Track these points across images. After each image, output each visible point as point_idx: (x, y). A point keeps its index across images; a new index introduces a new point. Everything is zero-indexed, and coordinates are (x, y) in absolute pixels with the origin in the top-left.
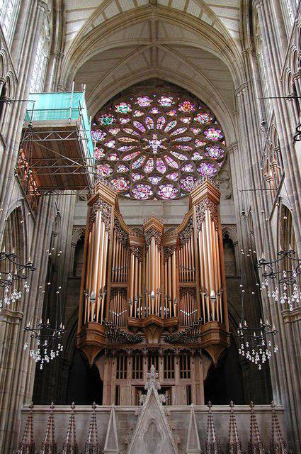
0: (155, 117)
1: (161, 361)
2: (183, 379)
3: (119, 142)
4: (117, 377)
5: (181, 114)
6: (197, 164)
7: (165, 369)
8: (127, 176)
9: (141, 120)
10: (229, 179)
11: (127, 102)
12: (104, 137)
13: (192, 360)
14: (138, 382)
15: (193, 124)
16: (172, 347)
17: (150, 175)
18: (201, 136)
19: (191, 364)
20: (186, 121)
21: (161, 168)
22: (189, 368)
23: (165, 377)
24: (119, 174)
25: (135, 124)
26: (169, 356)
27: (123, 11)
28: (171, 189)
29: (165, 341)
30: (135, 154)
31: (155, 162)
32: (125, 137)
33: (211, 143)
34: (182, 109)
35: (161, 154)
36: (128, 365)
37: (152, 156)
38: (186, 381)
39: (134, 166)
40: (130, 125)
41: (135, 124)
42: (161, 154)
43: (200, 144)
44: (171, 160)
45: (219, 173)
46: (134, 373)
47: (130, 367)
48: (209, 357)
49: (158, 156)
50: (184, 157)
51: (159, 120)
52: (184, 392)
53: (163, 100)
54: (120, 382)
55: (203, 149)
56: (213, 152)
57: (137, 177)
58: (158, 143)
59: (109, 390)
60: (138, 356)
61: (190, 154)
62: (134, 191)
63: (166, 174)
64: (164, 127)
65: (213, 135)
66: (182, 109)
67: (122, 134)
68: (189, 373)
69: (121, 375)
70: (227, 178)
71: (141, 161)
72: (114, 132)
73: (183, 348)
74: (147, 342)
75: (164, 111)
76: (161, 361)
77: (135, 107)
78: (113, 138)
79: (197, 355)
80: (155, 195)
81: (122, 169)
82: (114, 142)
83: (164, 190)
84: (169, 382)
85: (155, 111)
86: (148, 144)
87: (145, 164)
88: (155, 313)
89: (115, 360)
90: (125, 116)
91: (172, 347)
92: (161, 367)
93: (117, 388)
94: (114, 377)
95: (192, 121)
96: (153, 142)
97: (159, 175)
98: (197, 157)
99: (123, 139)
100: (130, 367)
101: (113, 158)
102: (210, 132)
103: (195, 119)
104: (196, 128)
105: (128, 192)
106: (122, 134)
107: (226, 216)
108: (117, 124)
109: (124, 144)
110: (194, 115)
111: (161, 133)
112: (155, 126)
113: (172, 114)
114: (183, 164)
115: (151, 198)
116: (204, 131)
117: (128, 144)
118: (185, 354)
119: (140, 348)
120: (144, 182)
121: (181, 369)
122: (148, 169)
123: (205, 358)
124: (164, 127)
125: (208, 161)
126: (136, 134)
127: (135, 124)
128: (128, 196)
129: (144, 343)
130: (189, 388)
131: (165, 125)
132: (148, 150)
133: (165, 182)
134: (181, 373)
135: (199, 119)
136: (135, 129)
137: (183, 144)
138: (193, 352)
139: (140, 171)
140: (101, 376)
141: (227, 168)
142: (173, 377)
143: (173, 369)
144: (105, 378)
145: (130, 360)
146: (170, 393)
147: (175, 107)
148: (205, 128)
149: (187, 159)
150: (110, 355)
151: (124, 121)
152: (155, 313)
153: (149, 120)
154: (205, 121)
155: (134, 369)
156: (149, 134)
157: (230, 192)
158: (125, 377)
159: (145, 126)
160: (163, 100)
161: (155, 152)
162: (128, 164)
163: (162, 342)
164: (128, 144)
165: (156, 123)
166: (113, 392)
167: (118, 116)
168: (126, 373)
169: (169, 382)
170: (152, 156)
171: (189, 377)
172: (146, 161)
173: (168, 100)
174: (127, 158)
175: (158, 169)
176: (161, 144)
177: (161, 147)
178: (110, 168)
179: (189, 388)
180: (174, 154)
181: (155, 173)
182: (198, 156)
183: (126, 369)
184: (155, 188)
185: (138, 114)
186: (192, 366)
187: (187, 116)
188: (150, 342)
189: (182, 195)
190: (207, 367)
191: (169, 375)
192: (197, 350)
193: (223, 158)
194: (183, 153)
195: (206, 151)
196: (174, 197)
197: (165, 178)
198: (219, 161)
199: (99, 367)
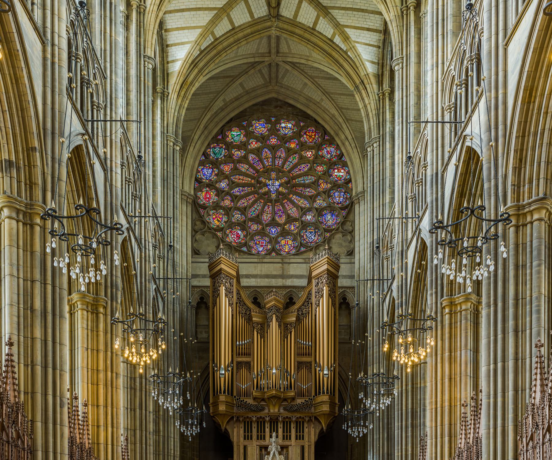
0: (273, 149)
1: (280, 425)
2: (298, 441)
3: (233, 183)
4: (245, 439)
5: (303, 146)
6: (320, 212)
7: (284, 432)
8: (243, 226)
9: (258, 152)
10: (352, 232)
11: (241, 127)
12: (216, 175)
13: (306, 425)
14: (262, 443)
15: (317, 159)
16: (289, 415)
17: (267, 225)
18: (327, 174)
19: (305, 428)
20: (309, 154)
22: (303, 432)
23: (284, 439)
24: (235, 223)
25: (251, 157)
26: (287, 423)
27: (236, 25)
28: (290, 242)
29: (285, 409)
30: (252, 198)
33: (336, 186)
34: (305, 138)
35: (281, 197)
36: (253, 429)
37: (271, 201)
38: (301, 442)
39: (252, 213)
40: (244, 159)
41: (250, 159)
42: (281, 197)
43: (323, 186)
44: (291, 206)
45: (343, 223)
46: (258, 436)
47: (254, 430)
48: (320, 422)
49: (277, 201)
50: (306, 202)
51: (279, 154)
52: (299, 451)
53: (283, 125)
54: (246, 443)
55: (327, 193)
56: (338, 197)
57: (255, 227)
58: (277, 183)
59: (239, 449)
60: (261, 423)
61: (312, 199)
62: (251, 244)
63: (285, 224)
64: (284, 164)
65: (339, 174)
66: (305, 138)
67: (236, 171)
68: (303, 436)
69: (248, 437)
70: (351, 228)
71: (258, 206)
72: (227, 169)
73: (299, 415)
74: (269, 411)
75: (284, 139)
76: (280, 425)
77: (249, 135)
78: (227, 177)
79: (310, 421)
80: (273, 250)
81: (237, 216)
83: (283, 242)
84: (287, 443)
85: (273, 141)
86: (267, 185)
87: (262, 211)
88: (275, 388)
89: (242, 425)
90: (239, 148)
91: (289, 415)
92: (280, 431)
93: (245, 448)
94: (242, 439)
95: (316, 157)
96: (270, 183)
97: (278, 225)
98: (320, 202)
99: (236, 179)
100: (254, 430)
101: (227, 202)
102: (336, 171)
104: (321, 165)
105: (245, 244)
106: (236, 171)
107: (345, 277)
108: (229, 158)
109: (238, 185)
110: (319, 147)
111: (280, 171)
112: (273, 161)
113: (293, 146)
114: (304, 211)
115: (269, 253)
116: (329, 168)
117: (244, 185)
118: (300, 420)
119: (263, 416)
120: (262, 233)
121: (297, 432)
122: (266, 217)
123: (317, 423)
124: (284, 164)
125: (331, 208)
126: (251, 171)
127: (251, 157)
128: (244, 249)
129: (266, 411)
130: (303, 448)
131: (286, 160)
132: (265, 194)
133: (285, 233)
134: (297, 436)
135: (325, 151)
136: (251, 166)
137: (305, 186)
138: (307, 419)
139: (257, 219)
140: (231, 437)
141: (351, 217)
142: (290, 439)
143: (290, 432)
144: (235, 440)
145: (254, 425)
146: (288, 451)
147: (297, 135)
148: (331, 165)
150: (238, 420)
151: (237, 154)
152: (275, 388)
153: (267, 153)
154: (331, 156)
155: (258, 432)
156: (267, 171)
157: (352, 246)
158: (251, 439)
159: (261, 160)
160: (283, 125)
161: (273, 196)
162: (243, 211)
163: (282, 411)
164: (244, 185)
165: (274, 158)
166: (242, 451)
167: (229, 146)
168: (251, 436)
169: (287, 443)
170: (271, 201)
171: (303, 439)
172: (264, 207)
173: (290, 125)
174: (243, 203)
175: (277, 218)
176: (280, 186)
177: (280, 189)
178: (224, 215)
179: (303, 448)
180: (294, 197)
181: (273, 223)
182: (321, 201)
183: (251, 432)
184: (274, 241)
185: (254, 145)
186: (306, 430)
187: (310, 148)
188: (272, 411)
189: (303, 249)
190: (317, 433)
191: (287, 437)
192: (310, 417)
193: (348, 205)
194: (305, 197)
195: (329, 196)
196: (293, 252)
197: (284, 228)
198: (343, 209)
199: (230, 430)
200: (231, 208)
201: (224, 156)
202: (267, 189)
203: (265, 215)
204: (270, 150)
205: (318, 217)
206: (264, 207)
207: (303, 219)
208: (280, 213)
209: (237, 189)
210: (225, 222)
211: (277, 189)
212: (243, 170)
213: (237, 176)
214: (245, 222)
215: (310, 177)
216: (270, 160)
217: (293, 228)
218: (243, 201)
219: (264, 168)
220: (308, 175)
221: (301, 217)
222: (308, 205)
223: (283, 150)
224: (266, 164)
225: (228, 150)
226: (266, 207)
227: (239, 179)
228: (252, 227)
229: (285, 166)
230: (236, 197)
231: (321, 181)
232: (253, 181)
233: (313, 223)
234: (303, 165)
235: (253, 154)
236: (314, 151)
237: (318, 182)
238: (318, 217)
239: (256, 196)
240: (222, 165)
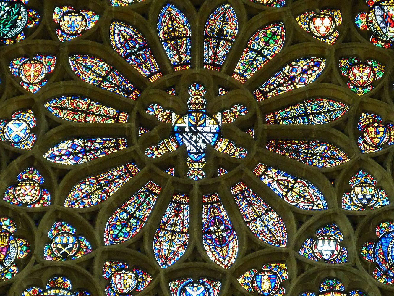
21: (222, 242)
24: (53, 266)
31: (196, 215)
32: (76, 96)
41: (116, 39)
44: (260, 206)
50: (314, 193)
63: (238, 270)
82: (29, 116)
96: (186, 122)
103: (361, 22)
149: (321, 204)
172: (160, 211)
176: (220, 134)
177: (222, 146)
178: (15, 236)
182: (370, 190)
200: (42, 213)
201: (25, 30)
202: (173, 147)
203: (164, 237)
204: (183, 11)
205: (360, 245)
206: (160, 211)
207: (305, 252)
208: (220, 231)
209: (65, 146)
210: (17, 262)
211: (209, 151)
212: (90, 79)
213: (67, 102)
214: (89, 263)
215: (327, 105)
216: (187, 44)
217: (266, 285)
218: (85, 187)
219: (163, 71)
220: (319, 98)
221: (298, 247)
222: (321, 204)
223: (231, 12)
224: (172, 57)
225: (39, 12)
226: (170, 211)
227: (76, 111)
228: (116, 280)
229: (239, 68)
230: (62, 172)
231: (366, 119)
232: (123, 118)
233: (342, 269)
234: (302, 64)
235: (127, 24)
236: (338, 15)
237: (357, 120)
238: (360, 245)
239: (133, 168)
240: (17, 63)
